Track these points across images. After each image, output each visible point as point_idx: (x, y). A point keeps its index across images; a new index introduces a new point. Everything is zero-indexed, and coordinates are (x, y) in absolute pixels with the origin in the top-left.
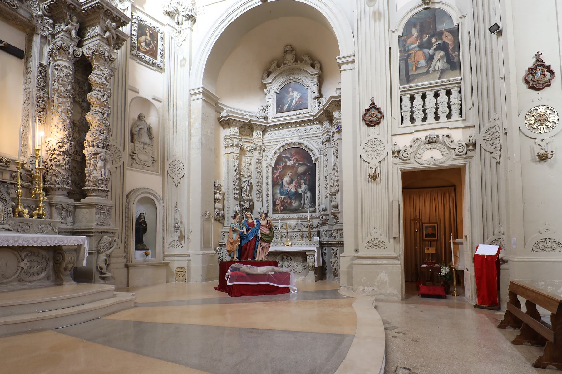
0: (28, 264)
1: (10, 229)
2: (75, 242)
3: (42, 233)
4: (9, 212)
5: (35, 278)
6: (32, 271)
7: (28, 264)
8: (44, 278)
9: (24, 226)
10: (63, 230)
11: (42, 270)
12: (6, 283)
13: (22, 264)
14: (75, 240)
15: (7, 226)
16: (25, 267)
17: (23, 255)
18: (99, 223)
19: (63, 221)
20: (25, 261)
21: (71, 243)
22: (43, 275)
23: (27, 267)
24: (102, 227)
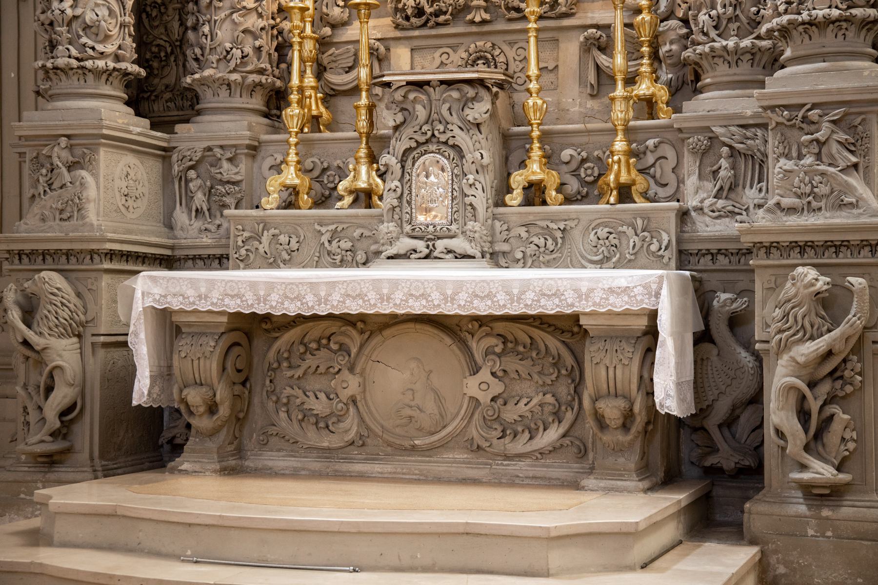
0: (497, 388)
1: (470, 252)
2: (612, 299)
3: (601, 263)
4: (468, 191)
5: (520, 445)
6: (510, 414)
7: (497, 388)
8: (554, 449)
9: (536, 240)
10: (714, 247)
11: (558, 417)
12: (430, 451)
13: (472, 386)
14: (611, 291)
15: (459, 244)
16: (485, 398)
17: (478, 347)
18: (787, 201)
19: (721, 203)
20: (485, 374)
21: (595, 304)
22: (552, 435)
23: (493, 399)
24: (793, 221)
